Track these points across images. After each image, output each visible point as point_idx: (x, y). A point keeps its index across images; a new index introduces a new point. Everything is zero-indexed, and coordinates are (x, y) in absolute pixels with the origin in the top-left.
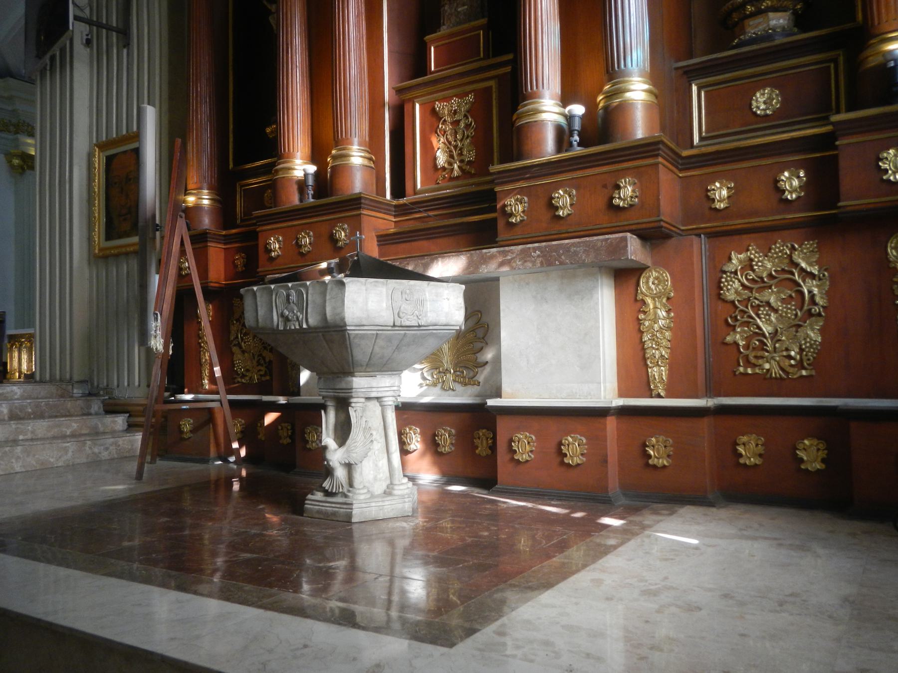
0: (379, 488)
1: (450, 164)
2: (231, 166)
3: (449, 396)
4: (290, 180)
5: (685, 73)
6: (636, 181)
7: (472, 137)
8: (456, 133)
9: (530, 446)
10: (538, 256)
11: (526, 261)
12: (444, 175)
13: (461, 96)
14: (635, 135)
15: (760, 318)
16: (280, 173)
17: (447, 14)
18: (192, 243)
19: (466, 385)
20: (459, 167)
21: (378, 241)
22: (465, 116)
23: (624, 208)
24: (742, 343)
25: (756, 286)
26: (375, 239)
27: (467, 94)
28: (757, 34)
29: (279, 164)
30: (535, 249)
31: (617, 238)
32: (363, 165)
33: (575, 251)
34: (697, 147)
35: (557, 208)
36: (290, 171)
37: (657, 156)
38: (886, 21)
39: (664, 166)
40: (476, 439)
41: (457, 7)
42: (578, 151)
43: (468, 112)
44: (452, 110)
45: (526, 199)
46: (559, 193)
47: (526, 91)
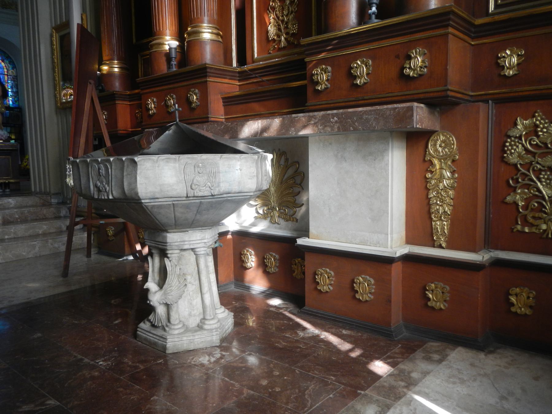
0: (193, 322)
1: (279, 36)
2: (134, 41)
3: (276, 228)
4: (160, 53)
6: (426, 52)
8: (283, 9)
9: (330, 280)
10: (336, 122)
11: (326, 126)
12: (274, 46)
14: (428, 5)
15: (541, 182)
16: (154, 47)
18: (100, 103)
19: (287, 221)
20: (285, 39)
21: (223, 102)
23: (413, 78)
24: (521, 204)
25: (539, 151)
26: (221, 101)
30: (333, 116)
31: (404, 108)
32: (211, 40)
33: (366, 119)
34: (493, 14)
35: (355, 77)
36: (160, 46)
37: (447, 26)
39: (454, 35)
40: (293, 265)
42: (375, 23)
45: (329, 68)
46: (357, 64)
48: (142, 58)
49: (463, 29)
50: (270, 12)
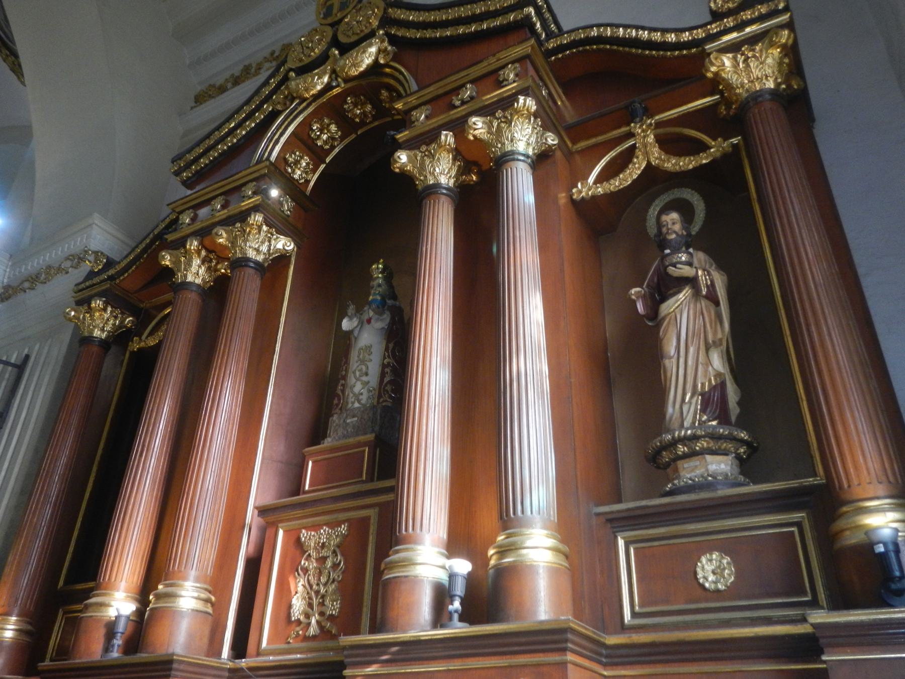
1: (308, 616)
2: (61, 583)
4: (98, 620)
5: (610, 521)
7: (339, 582)
8: (320, 573)
12: (298, 632)
13: (333, 525)
14: (535, 613)
16: (90, 609)
17: (335, 425)
20: (318, 622)
28: (693, 481)
29: (94, 596)
32: (193, 610)
36: (103, 608)
37: (564, 650)
38: (859, 484)
39: (575, 664)
41: (346, 417)
42: (458, 628)
43: (338, 546)
44: (319, 543)
47: (399, 532)
48: (65, 616)
49: (588, 654)
50: (299, 574)
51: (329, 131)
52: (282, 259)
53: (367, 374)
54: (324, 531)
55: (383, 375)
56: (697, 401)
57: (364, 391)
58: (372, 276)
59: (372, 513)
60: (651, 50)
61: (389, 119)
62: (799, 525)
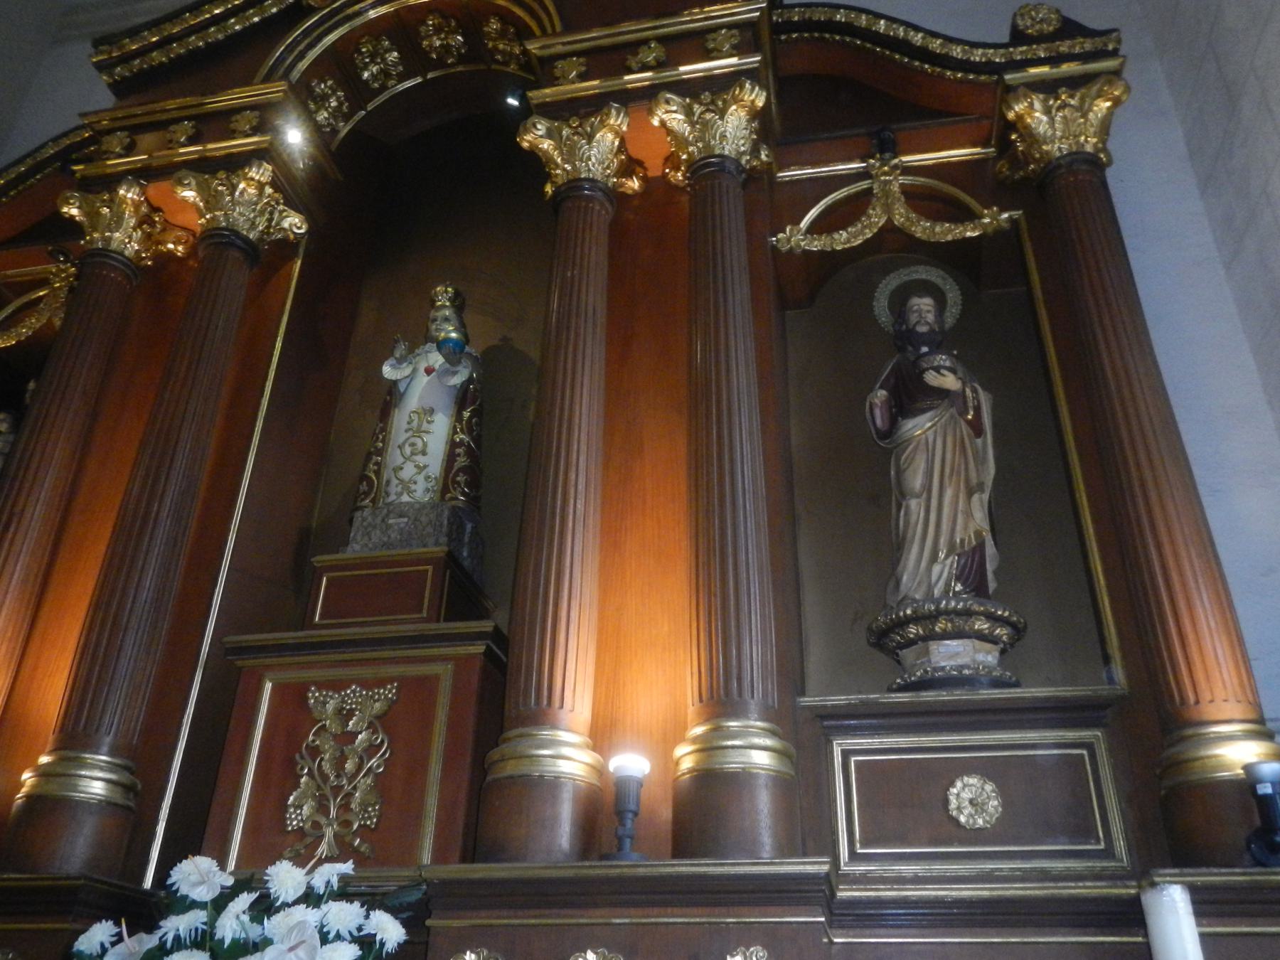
7: (377, 775)
20: (336, 835)
22: (370, 725)
27: (381, 683)
41: (387, 515)
50: (302, 757)
51: (384, 60)
52: (285, 247)
53: (424, 453)
54: (354, 692)
55: (450, 458)
56: (952, 562)
57: (420, 478)
58: (433, 302)
59: (444, 671)
60: (923, 61)
61: (482, 67)
62: (1089, 747)
